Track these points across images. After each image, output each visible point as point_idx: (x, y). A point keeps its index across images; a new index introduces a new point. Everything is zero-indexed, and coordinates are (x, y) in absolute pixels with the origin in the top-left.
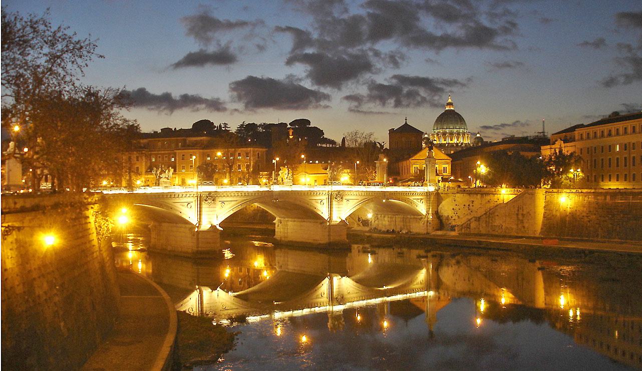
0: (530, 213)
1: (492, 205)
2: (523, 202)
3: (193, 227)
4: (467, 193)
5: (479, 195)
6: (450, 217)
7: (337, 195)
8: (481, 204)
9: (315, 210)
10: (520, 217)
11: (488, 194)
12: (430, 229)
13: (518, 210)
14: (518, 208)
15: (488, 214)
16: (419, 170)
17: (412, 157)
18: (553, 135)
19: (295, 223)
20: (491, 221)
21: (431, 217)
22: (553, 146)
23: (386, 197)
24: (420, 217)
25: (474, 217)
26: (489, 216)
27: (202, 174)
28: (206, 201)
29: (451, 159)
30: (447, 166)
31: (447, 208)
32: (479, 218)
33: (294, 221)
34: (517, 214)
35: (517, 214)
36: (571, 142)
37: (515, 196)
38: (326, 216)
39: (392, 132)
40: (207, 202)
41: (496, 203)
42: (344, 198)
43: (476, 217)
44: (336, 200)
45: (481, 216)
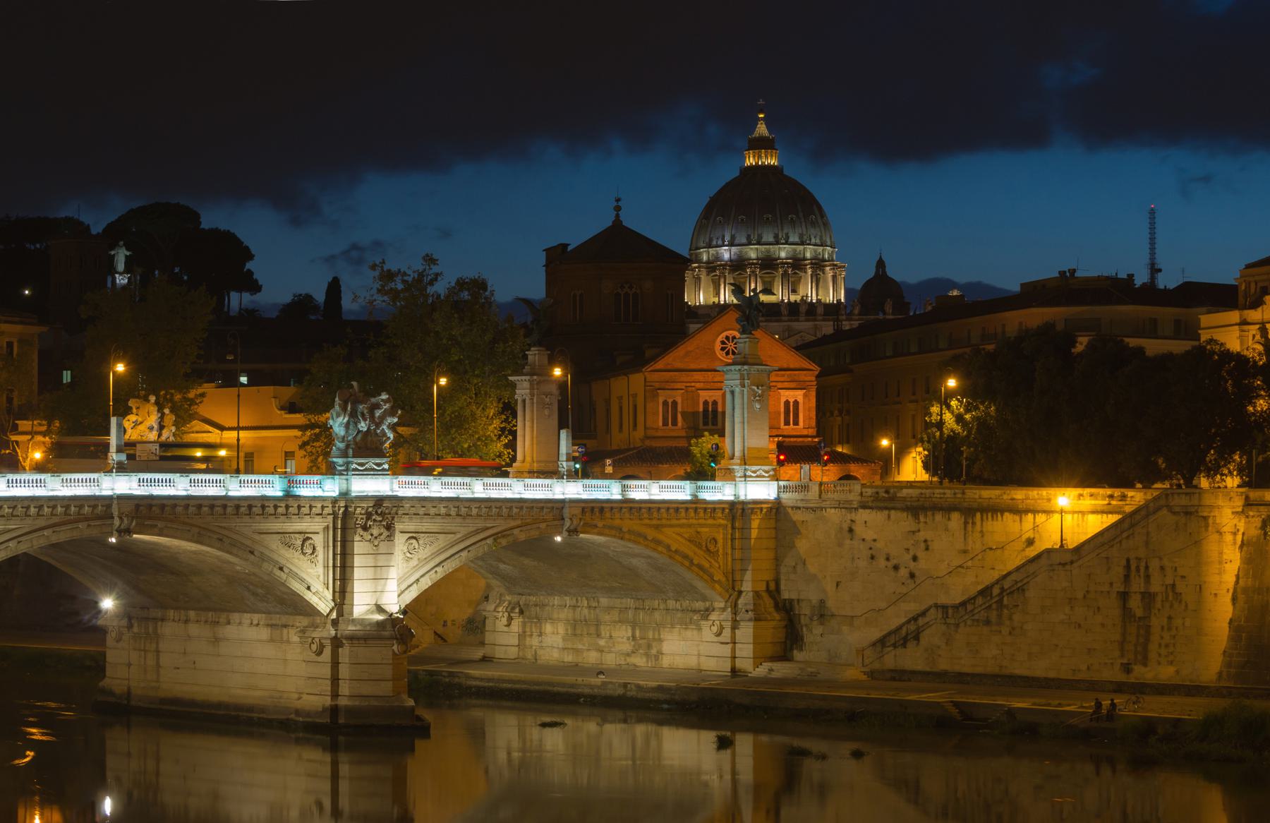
0: (1178, 590)
1: (1013, 559)
2: (1147, 543)
4: (907, 509)
5: (955, 516)
7: (369, 516)
8: (965, 552)
10: (1135, 603)
11: (995, 510)
13: (1127, 577)
14: (1128, 566)
15: (996, 591)
16: (683, 413)
17: (654, 358)
18: (1248, 266)
22: (1254, 315)
23: (567, 523)
25: (936, 606)
26: (1000, 602)
29: (817, 369)
30: (799, 395)
32: (956, 607)
34: (1124, 596)
35: (1124, 596)
37: (1113, 518)
38: (322, 601)
39: (557, 257)
41: (1032, 552)
42: (398, 526)
43: (944, 608)
44: (367, 536)
45: (963, 604)
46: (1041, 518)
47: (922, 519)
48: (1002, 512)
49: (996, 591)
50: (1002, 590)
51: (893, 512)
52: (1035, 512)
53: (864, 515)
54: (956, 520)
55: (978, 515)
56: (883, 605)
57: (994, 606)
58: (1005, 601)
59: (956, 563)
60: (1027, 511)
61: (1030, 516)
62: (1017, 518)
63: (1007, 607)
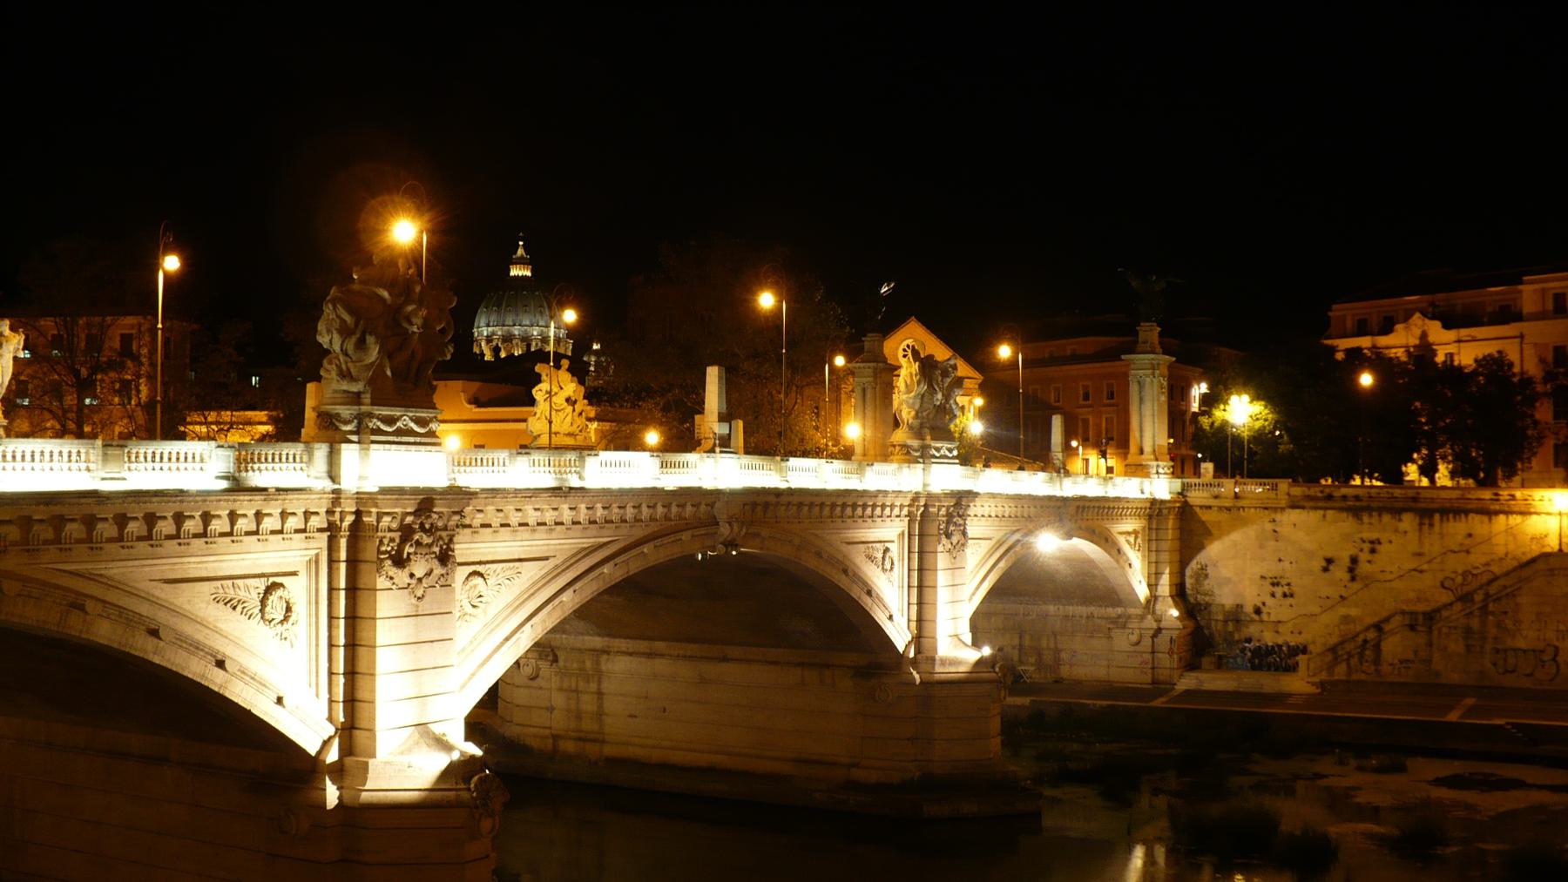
3: (304, 768)
4: (1348, 509)
6: (1249, 609)
8: (1420, 554)
9: (867, 602)
12: (1167, 662)
15: (1478, 597)
19: (660, 665)
20: (1493, 631)
21: (1175, 613)
24: (1113, 612)
25: (1403, 613)
26: (1486, 606)
27: (373, 353)
28: (400, 561)
29: (980, 378)
31: (1236, 567)
33: (650, 655)
36: (1490, 324)
40: (402, 577)
46: (1515, 520)
47: (1366, 519)
48: (1467, 512)
49: (1478, 597)
50: (1487, 595)
51: (1330, 513)
52: (1508, 513)
53: (1294, 516)
54: (1408, 522)
55: (1437, 517)
56: (1317, 610)
57: (1477, 613)
58: (1491, 607)
59: (1409, 566)
60: (1497, 513)
61: (1502, 517)
62: (1485, 519)
63: (1492, 613)
